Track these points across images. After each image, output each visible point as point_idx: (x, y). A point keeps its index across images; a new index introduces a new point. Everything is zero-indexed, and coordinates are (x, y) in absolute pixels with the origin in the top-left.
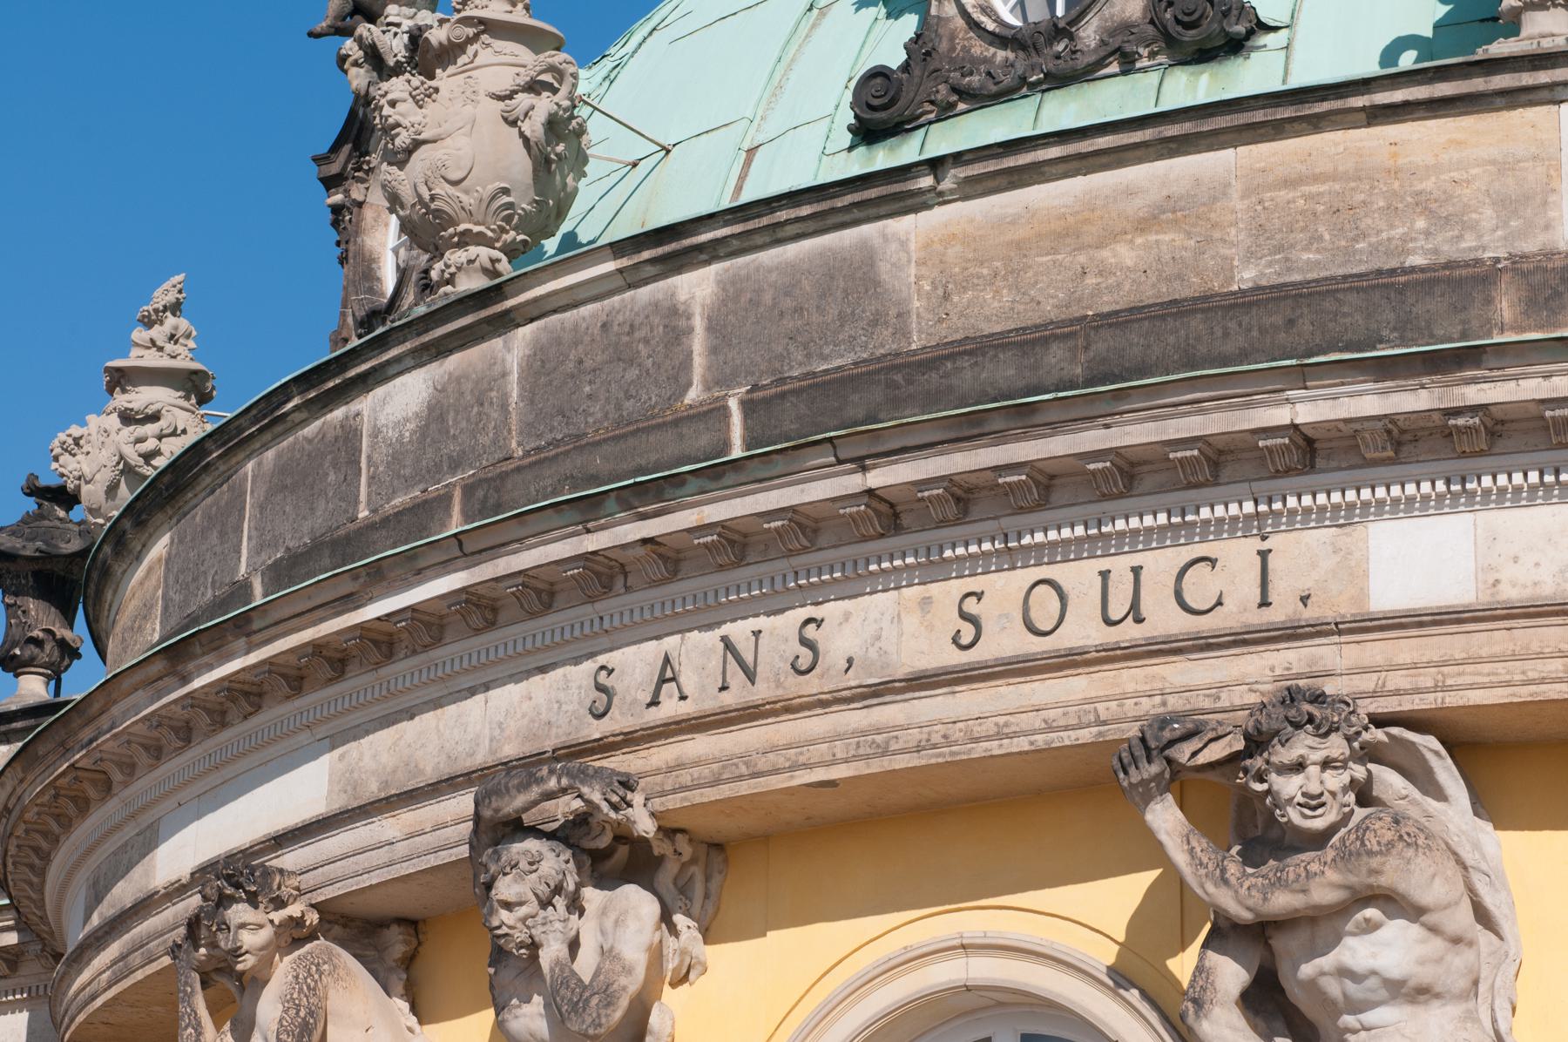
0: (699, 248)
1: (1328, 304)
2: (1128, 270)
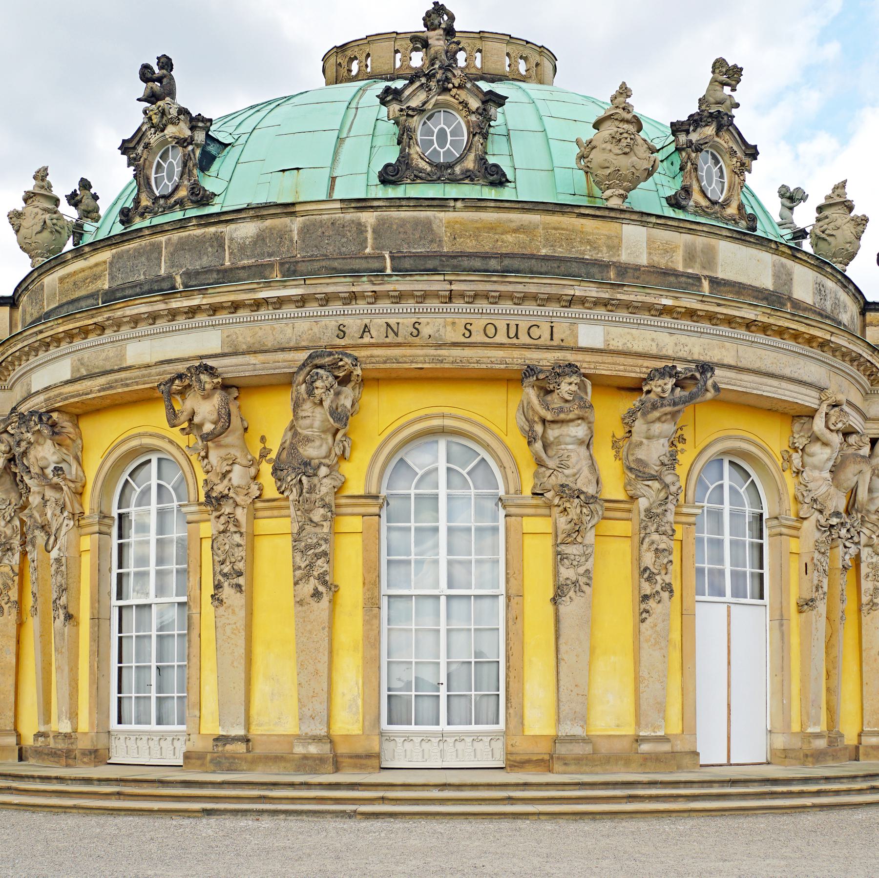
0: (372, 207)
1: (568, 264)
2: (510, 242)
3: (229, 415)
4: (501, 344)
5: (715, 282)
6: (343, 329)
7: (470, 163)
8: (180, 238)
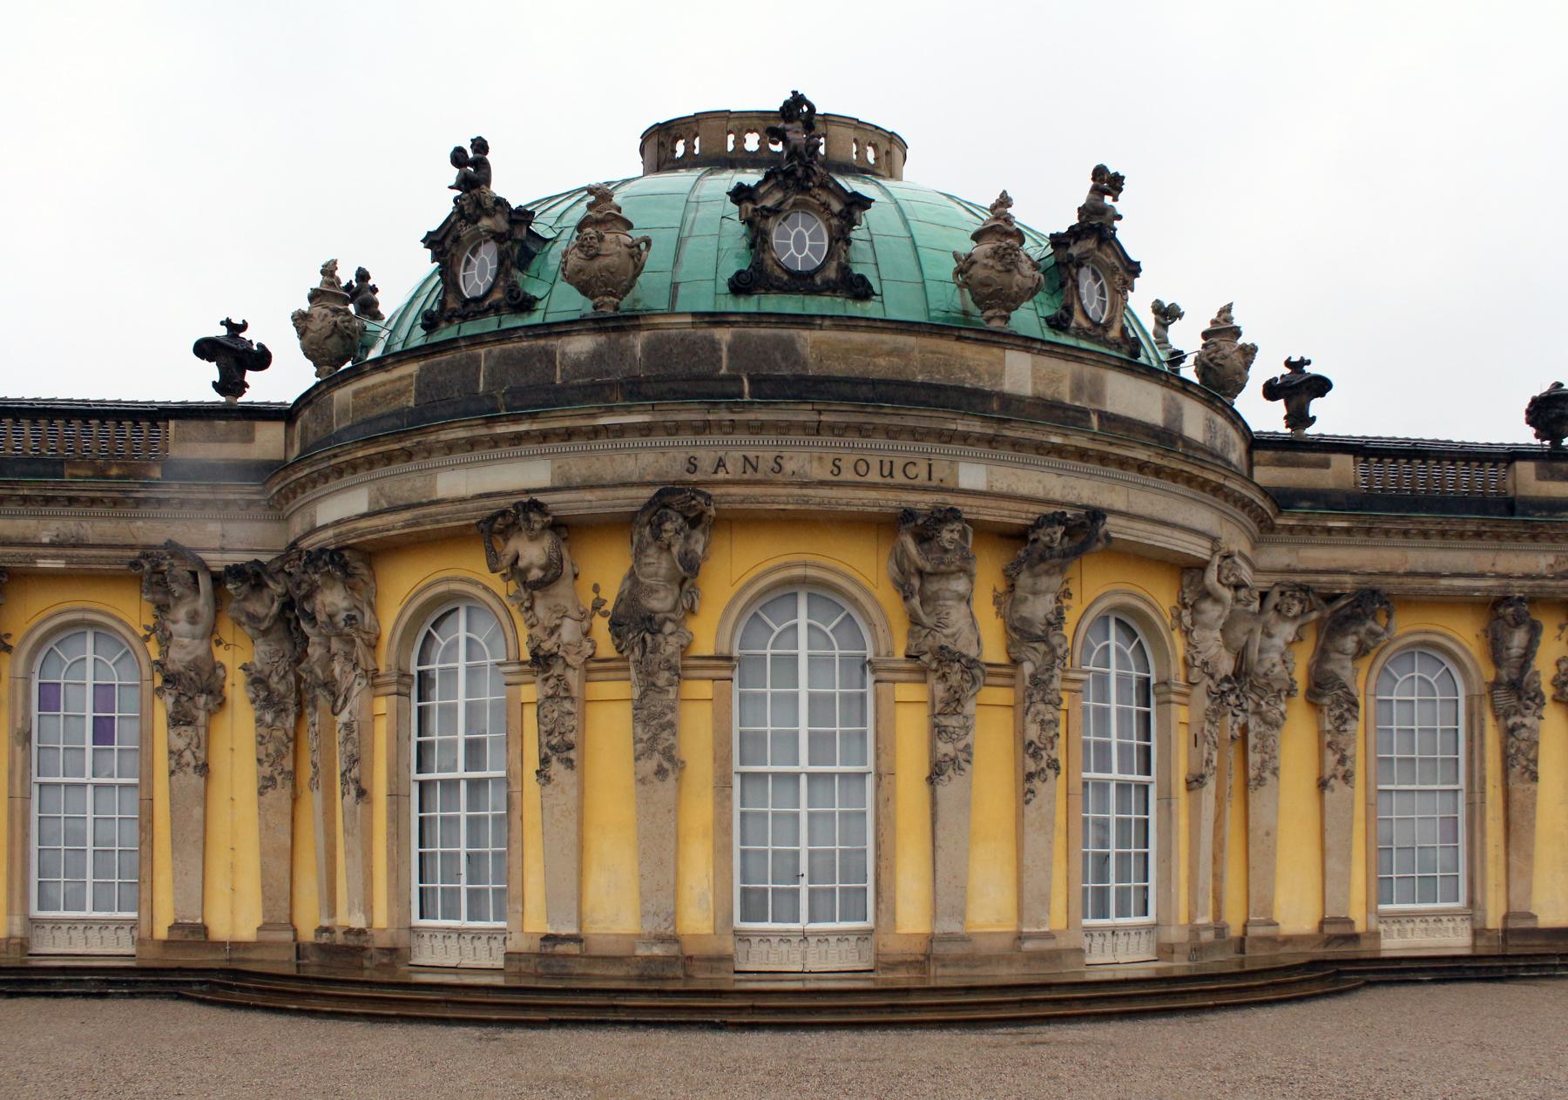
2: (882, 366)
3: (561, 560)
5: (1105, 417)
7: (832, 273)
8: (503, 351)
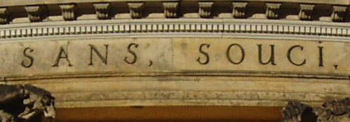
4: (251, 72)
6: (31, 54)
